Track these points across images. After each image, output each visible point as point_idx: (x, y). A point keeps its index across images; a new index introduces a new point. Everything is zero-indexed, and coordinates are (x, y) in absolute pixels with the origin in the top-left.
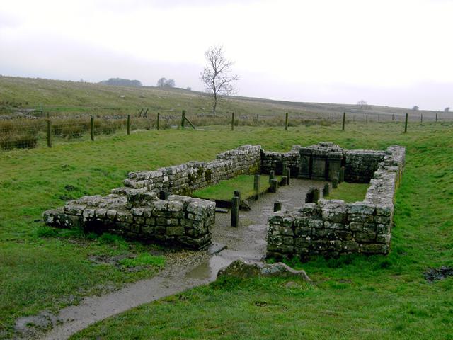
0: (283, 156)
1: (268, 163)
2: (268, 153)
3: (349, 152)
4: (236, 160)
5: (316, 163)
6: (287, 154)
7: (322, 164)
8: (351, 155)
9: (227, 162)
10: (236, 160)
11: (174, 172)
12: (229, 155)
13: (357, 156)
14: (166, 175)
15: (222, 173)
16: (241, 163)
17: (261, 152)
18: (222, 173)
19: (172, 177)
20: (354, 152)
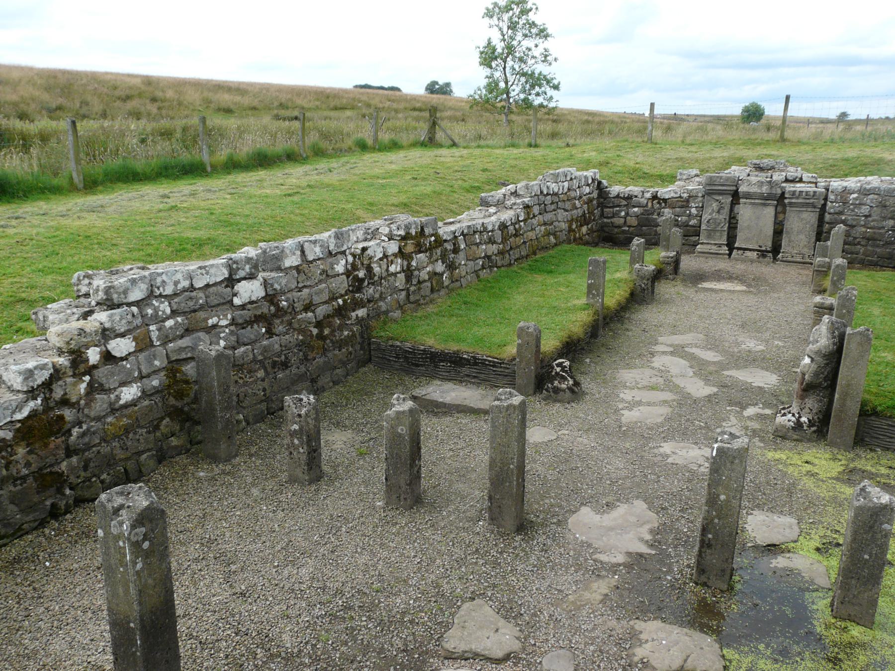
0: (655, 197)
1: (614, 215)
2: (615, 189)
3: (836, 184)
4: (536, 209)
5: (745, 212)
6: (666, 191)
7: (770, 212)
8: (846, 191)
9: (507, 216)
10: (536, 209)
11: (292, 261)
12: (515, 194)
13: (864, 192)
14: (251, 277)
15: (493, 249)
16: (548, 217)
17: (600, 183)
18: (493, 249)
19: (280, 281)
20: (852, 183)
